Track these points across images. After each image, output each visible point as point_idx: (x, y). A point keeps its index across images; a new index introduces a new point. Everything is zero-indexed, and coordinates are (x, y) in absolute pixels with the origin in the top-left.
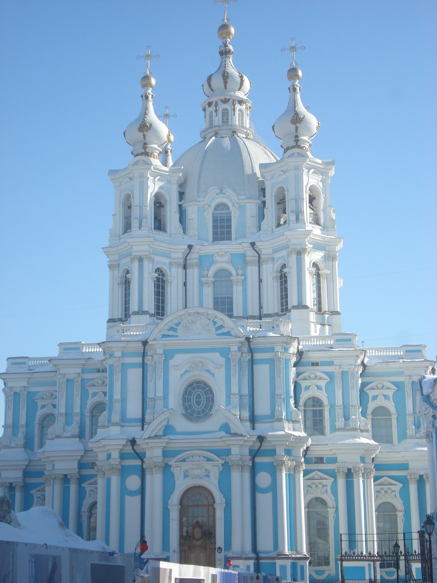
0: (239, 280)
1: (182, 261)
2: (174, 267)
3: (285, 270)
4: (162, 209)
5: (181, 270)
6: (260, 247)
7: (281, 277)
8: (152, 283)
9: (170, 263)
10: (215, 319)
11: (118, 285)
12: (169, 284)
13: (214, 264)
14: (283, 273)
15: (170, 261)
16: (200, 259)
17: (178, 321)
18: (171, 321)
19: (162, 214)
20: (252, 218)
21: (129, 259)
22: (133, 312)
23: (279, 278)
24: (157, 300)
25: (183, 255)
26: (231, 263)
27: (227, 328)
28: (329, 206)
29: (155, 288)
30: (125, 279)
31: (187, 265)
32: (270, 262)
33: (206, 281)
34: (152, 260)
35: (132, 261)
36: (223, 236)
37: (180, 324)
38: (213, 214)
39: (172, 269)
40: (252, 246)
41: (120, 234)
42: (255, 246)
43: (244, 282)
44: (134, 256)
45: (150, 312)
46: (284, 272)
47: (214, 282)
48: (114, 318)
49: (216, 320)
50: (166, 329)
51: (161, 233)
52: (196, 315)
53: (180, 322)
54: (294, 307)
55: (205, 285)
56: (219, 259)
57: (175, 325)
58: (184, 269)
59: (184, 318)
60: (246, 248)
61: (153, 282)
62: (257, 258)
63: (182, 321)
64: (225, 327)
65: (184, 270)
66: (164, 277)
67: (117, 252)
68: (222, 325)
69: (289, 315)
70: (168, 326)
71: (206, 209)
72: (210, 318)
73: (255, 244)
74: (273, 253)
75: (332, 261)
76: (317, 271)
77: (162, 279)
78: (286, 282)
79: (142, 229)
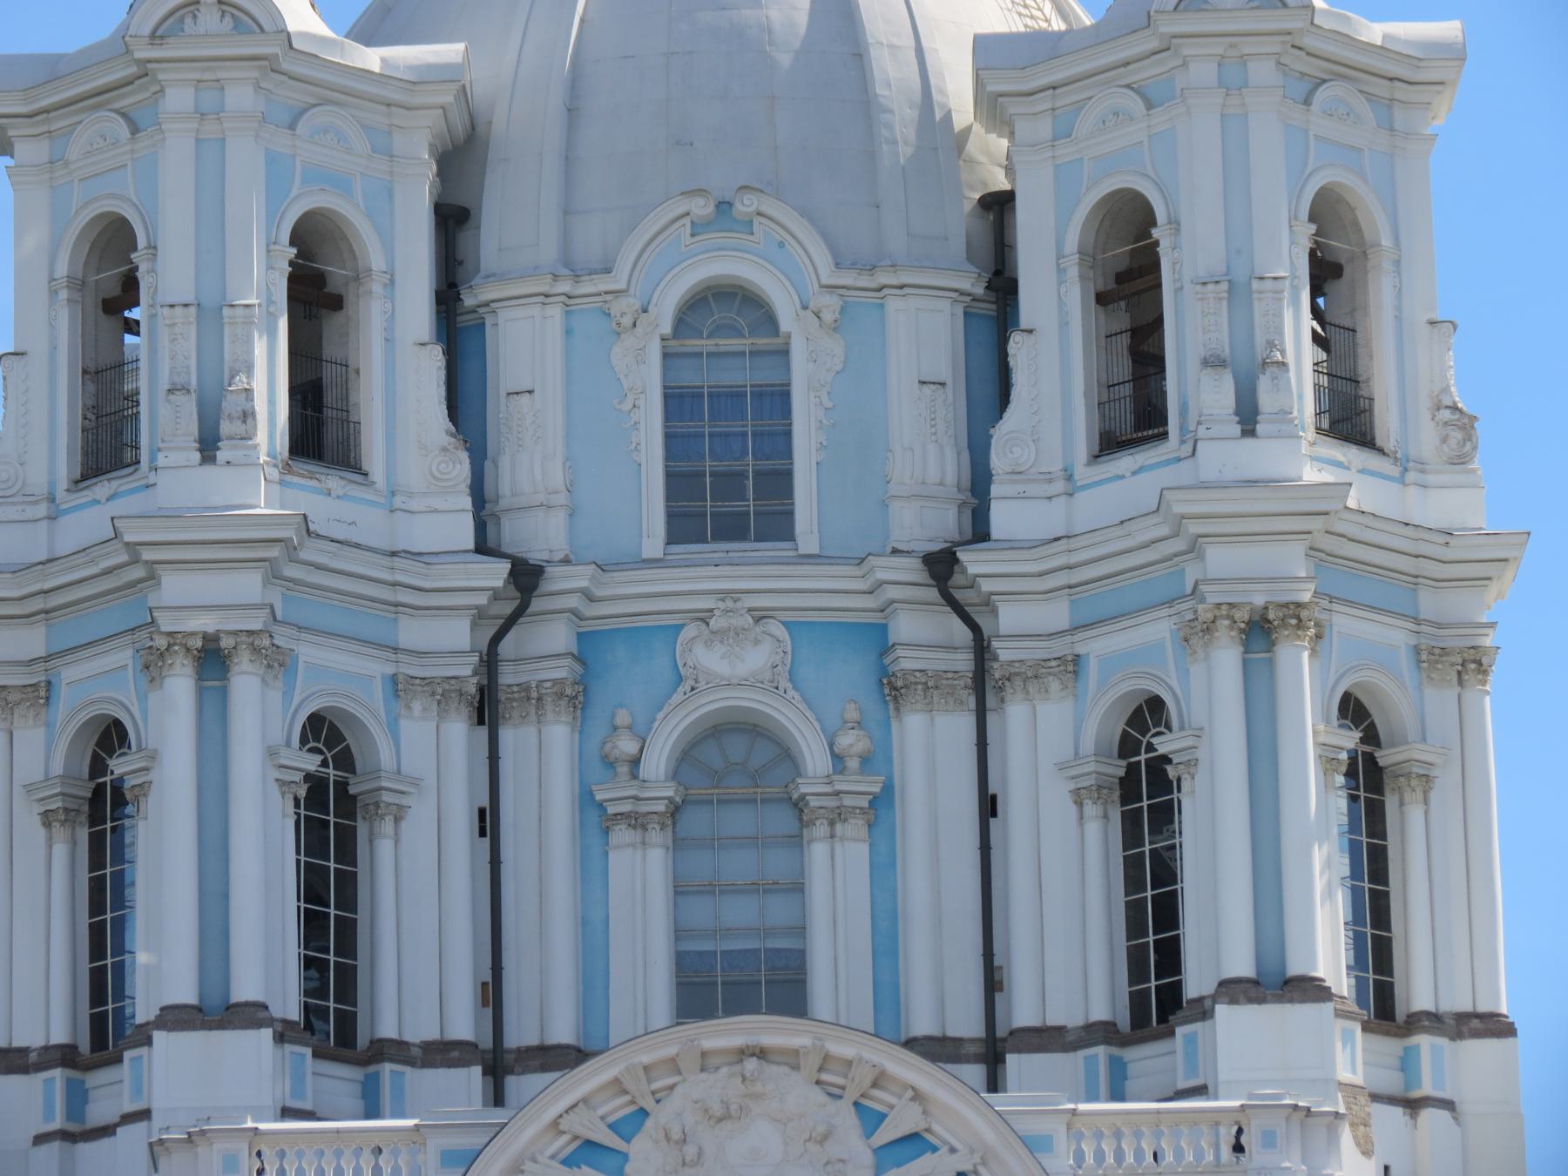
0: (848, 801)
1: (468, 671)
2: (417, 706)
3: (1164, 745)
4: (332, 324)
5: (459, 730)
6: (986, 586)
7: (1128, 788)
8: (284, 815)
9: (394, 679)
10: (876, 1093)
11: (47, 824)
12: (387, 826)
13: (681, 689)
14: (1143, 757)
15: (390, 669)
16: (579, 659)
17: (633, 1102)
18: (585, 1100)
19: (330, 350)
20: (927, 390)
21: (129, 652)
22: (162, 1009)
23: (1117, 793)
24: (313, 926)
25: (474, 626)
26: (795, 688)
27: (953, 1150)
28: (1432, 323)
29: (298, 853)
30: (92, 785)
31: (502, 696)
32: (1055, 685)
33: (626, 807)
34: (277, 662)
35: (153, 664)
36: (736, 506)
37: (642, 1124)
38: (666, 356)
39: (405, 726)
40: (933, 576)
41: (52, 484)
42: (957, 579)
43: (881, 807)
44: (170, 634)
45: (276, 1011)
46: (1150, 748)
47: (675, 811)
48: (16, 1044)
49: (882, 1099)
50: (552, 1157)
51: (334, 481)
52: (751, 1064)
53: (644, 1113)
54: (1234, 990)
55: (621, 834)
56: (710, 659)
57: (611, 1127)
58: (481, 722)
59: (672, 1088)
60: (892, 593)
61: (291, 809)
62: (964, 662)
63: (658, 1101)
64: (935, 1149)
65: (483, 732)
66: (353, 771)
67: (38, 604)
68: (914, 1137)
69: (1191, 1040)
70: (565, 1138)
71: (627, 321)
72: (843, 1088)
73: (957, 561)
74: (1074, 629)
75: (1461, 682)
76: (1367, 749)
77: (342, 786)
78: (1165, 816)
79: (221, 456)
